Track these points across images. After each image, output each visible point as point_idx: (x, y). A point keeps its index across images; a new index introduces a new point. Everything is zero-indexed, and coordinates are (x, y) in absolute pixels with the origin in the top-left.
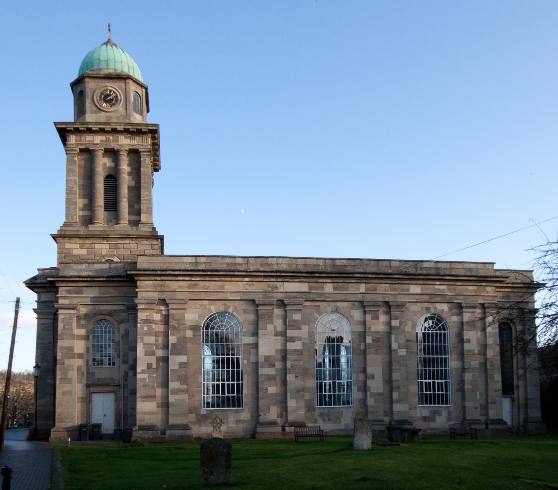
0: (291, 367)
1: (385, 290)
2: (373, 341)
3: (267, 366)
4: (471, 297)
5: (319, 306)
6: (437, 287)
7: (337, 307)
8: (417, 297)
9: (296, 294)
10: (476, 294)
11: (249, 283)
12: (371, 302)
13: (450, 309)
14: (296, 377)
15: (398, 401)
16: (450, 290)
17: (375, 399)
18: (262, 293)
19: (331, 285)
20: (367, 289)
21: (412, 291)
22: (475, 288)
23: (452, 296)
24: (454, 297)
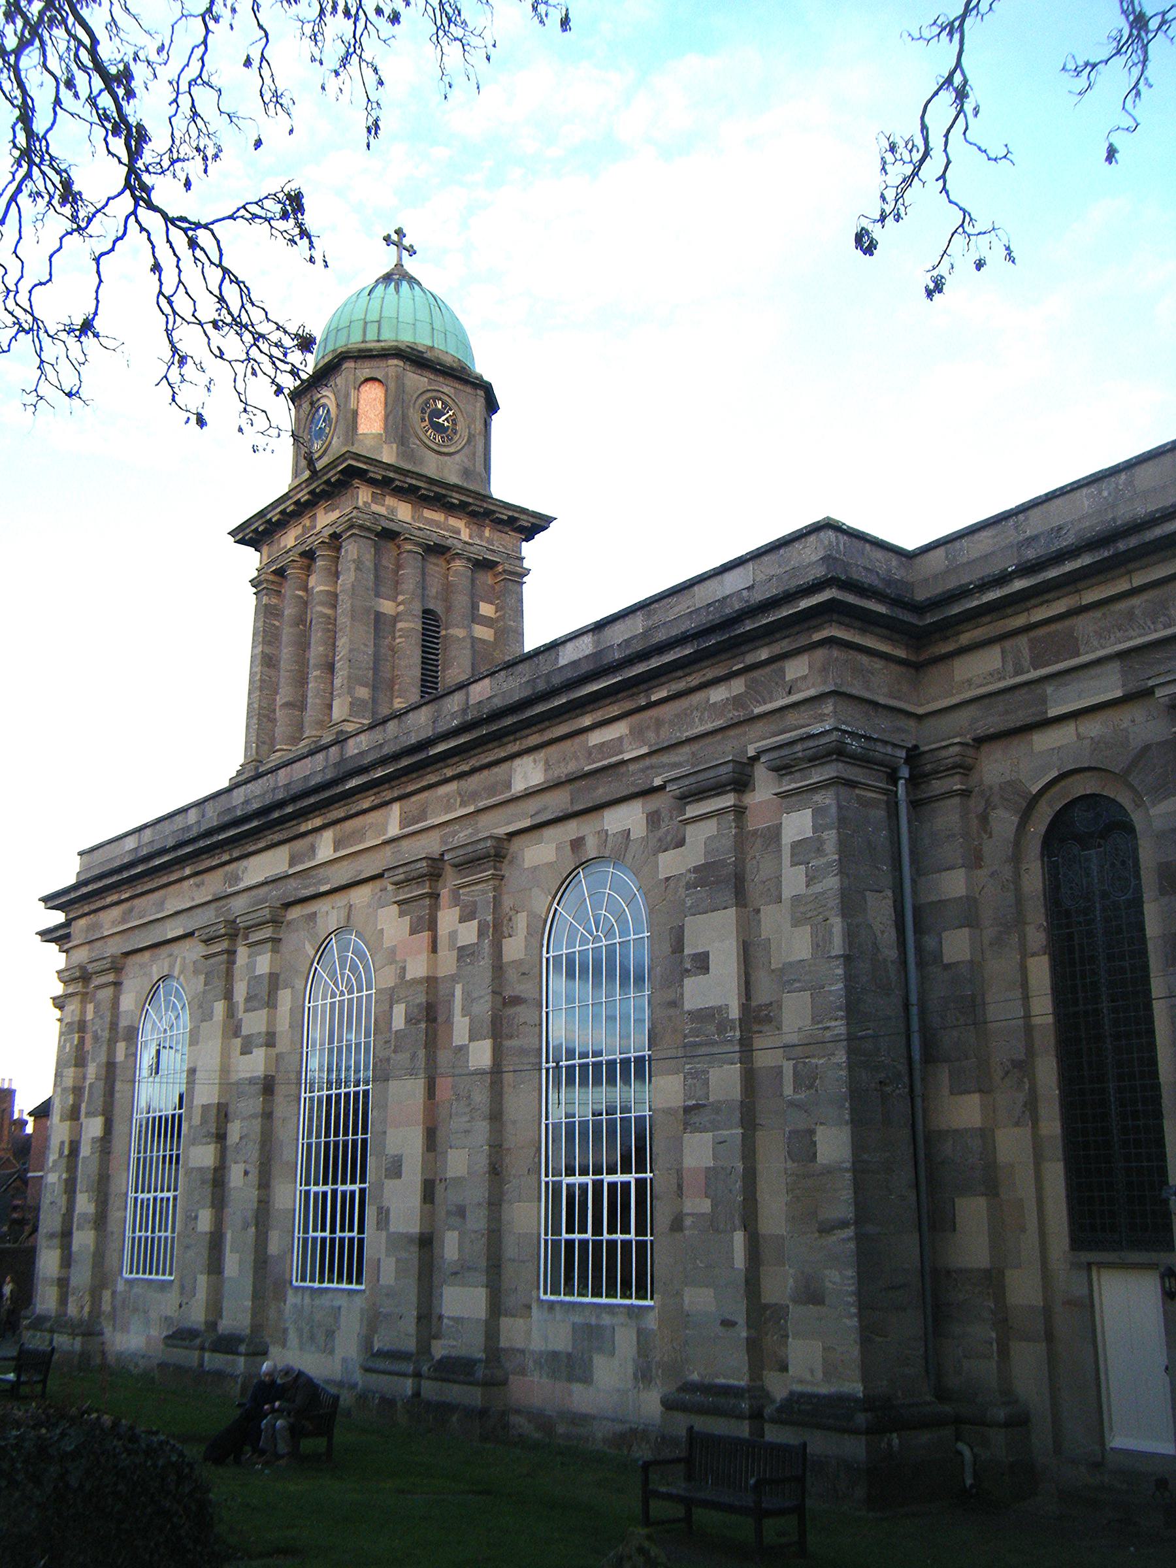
0: (241, 1138)
1: (449, 808)
2: (409, 1020)
3: (204, 1140)
4: (719, 737)
5: (315, 913)
6: (596, 738)
7: (351, 906)
8: (532, 805)
9: (265, 889)
10: (741, 714)
11: (198, 879)
12: (401, 870)
13: (653, 819)
14: (246, 1173)
15: (456, 1273)
16: (637, 734)
17: (398, 1261)
18: (213, 905)
19: (328, 835)
20: (404, 822)
21: (518, 786)
22: (738, 686)
23: (647, 762)
24: (654, 760)
